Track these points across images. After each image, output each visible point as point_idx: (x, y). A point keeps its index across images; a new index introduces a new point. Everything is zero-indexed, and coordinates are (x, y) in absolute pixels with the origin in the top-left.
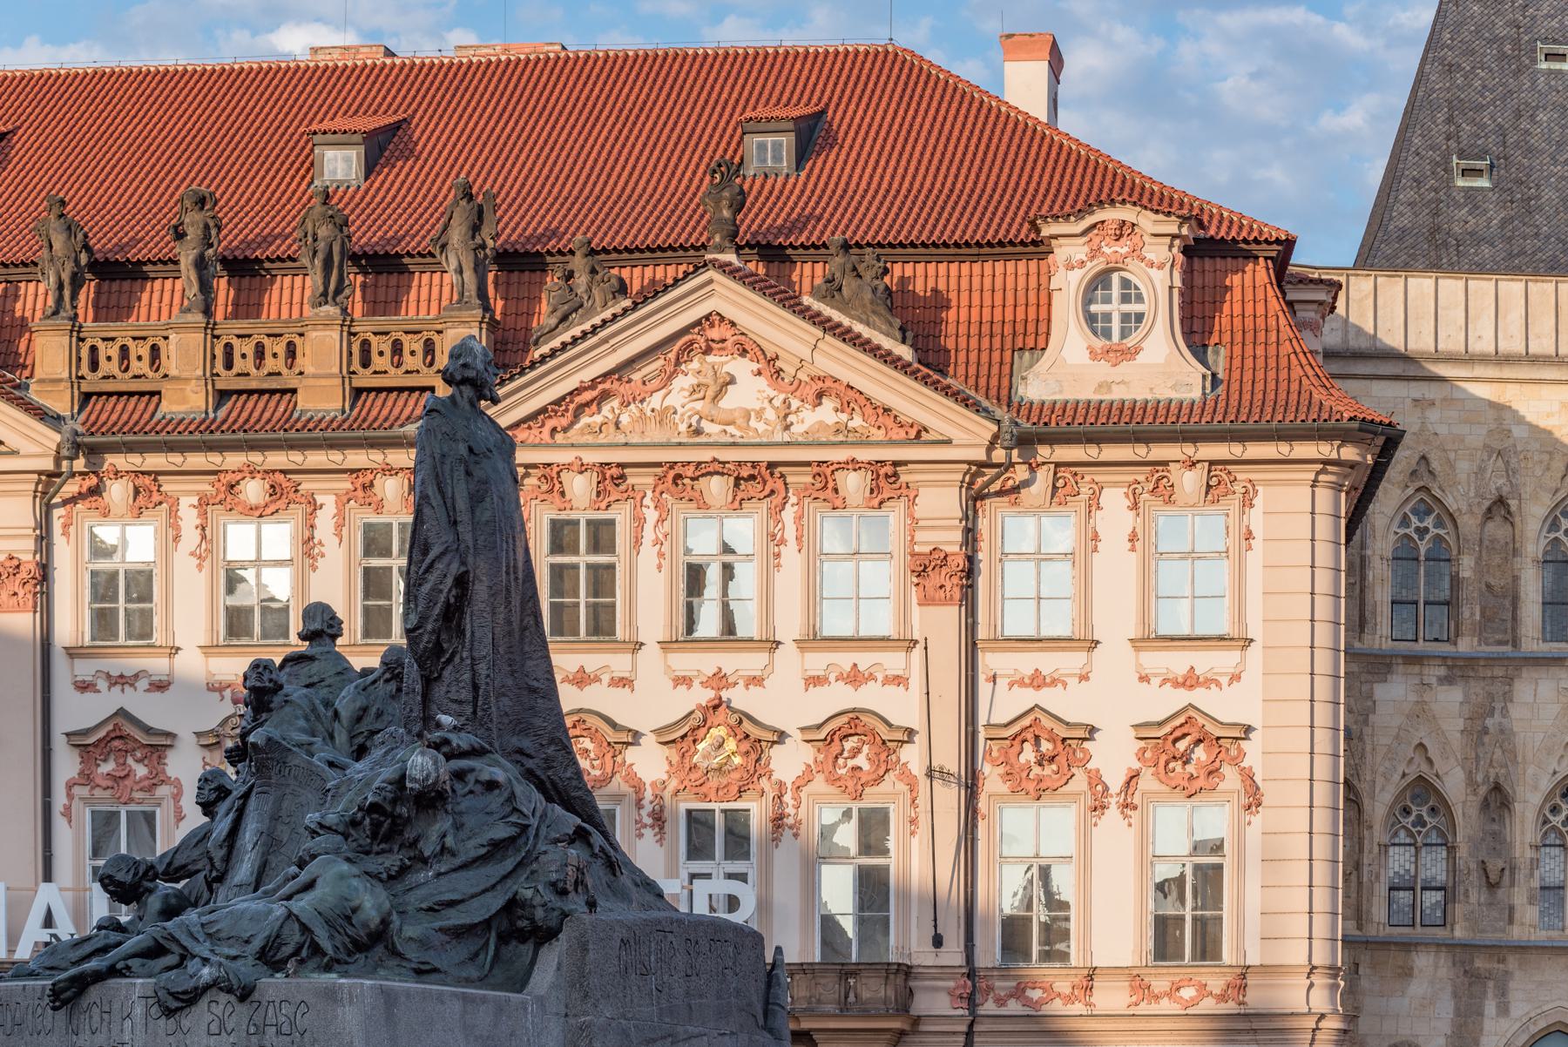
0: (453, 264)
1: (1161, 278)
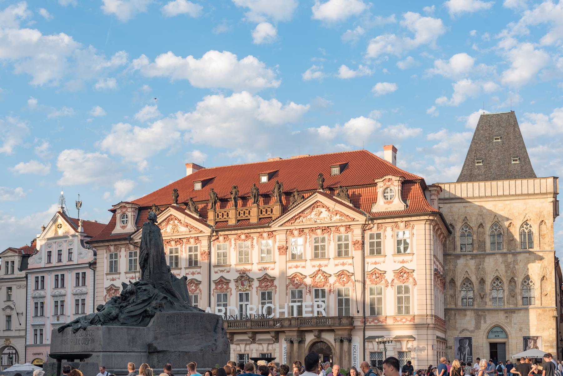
0: (276, 195)
1: (397, 188)
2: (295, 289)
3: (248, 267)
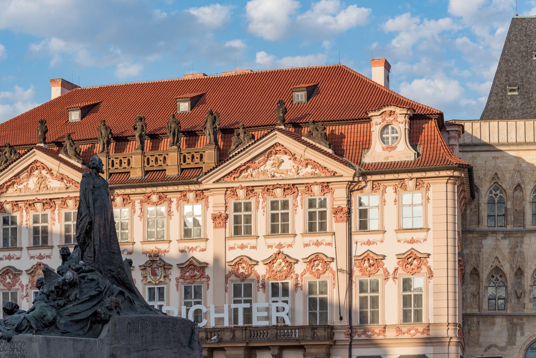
1: (402, 126)
2: (239, 283)
3: (162, 247)
